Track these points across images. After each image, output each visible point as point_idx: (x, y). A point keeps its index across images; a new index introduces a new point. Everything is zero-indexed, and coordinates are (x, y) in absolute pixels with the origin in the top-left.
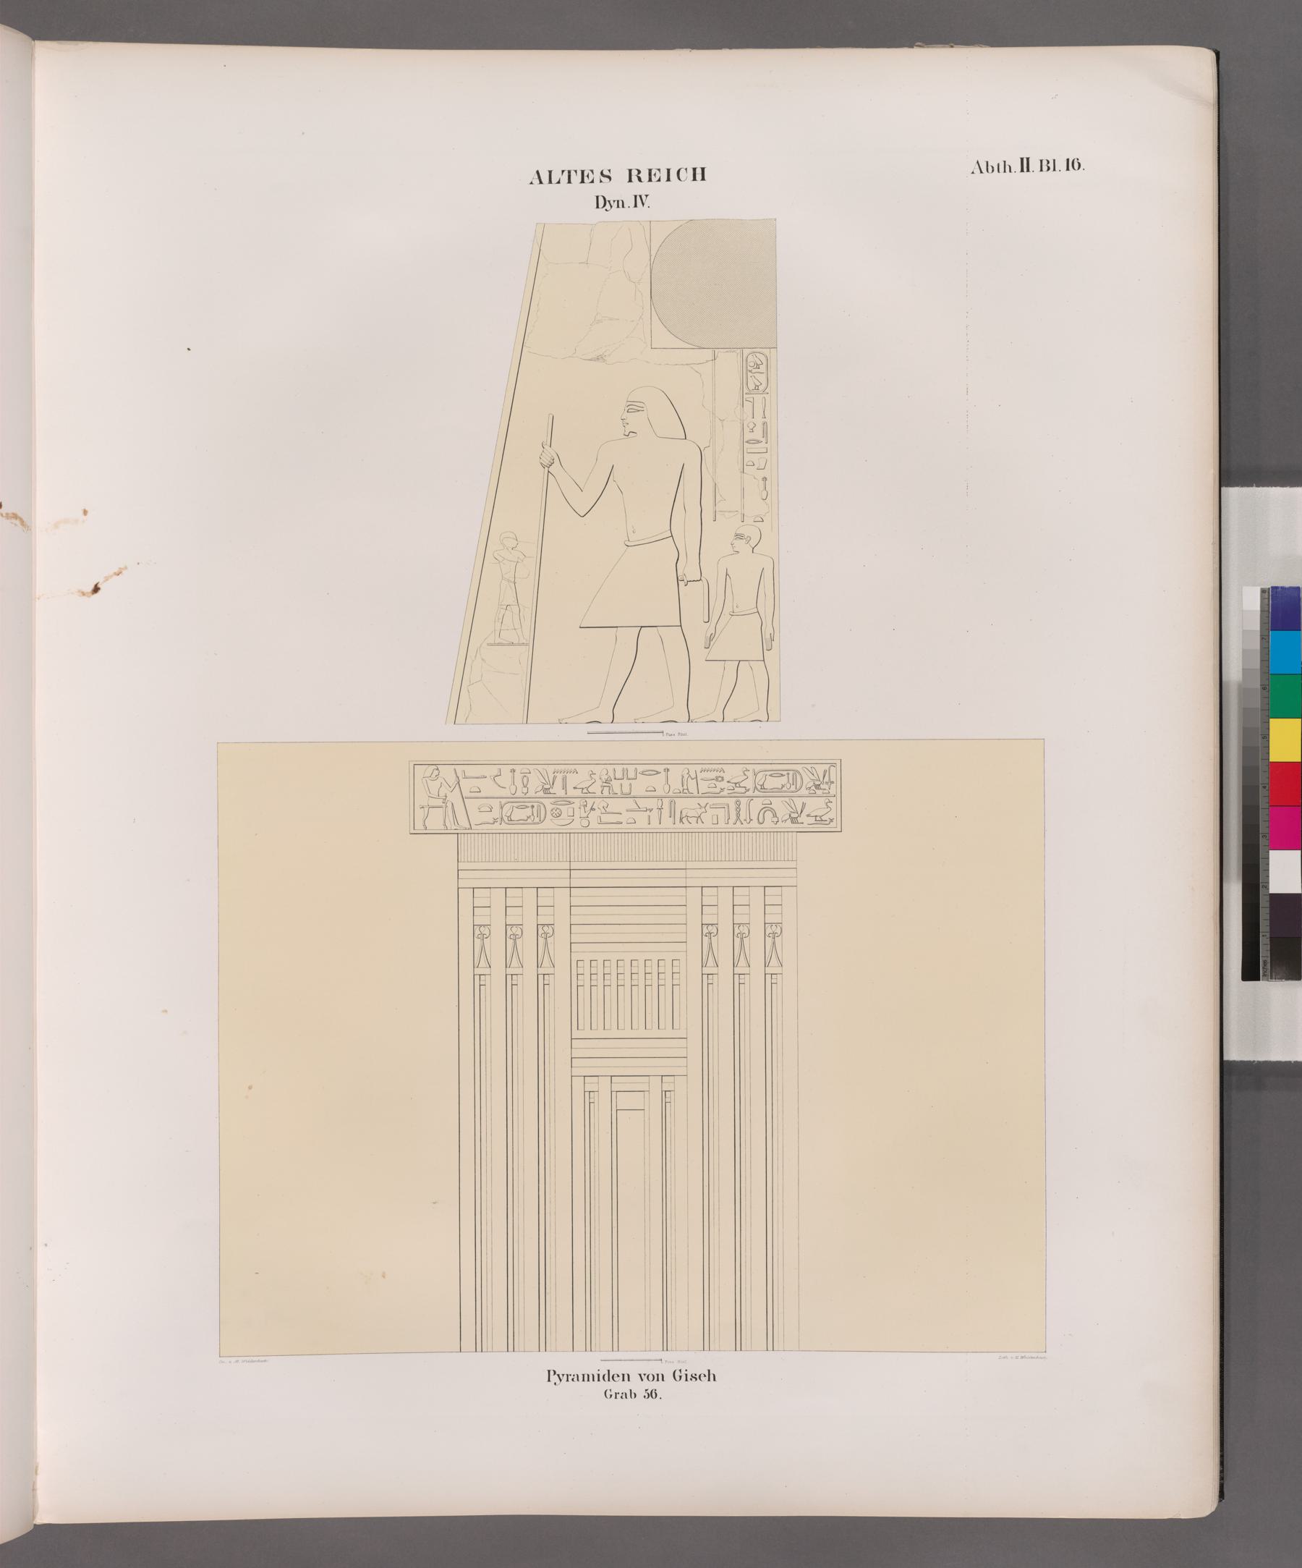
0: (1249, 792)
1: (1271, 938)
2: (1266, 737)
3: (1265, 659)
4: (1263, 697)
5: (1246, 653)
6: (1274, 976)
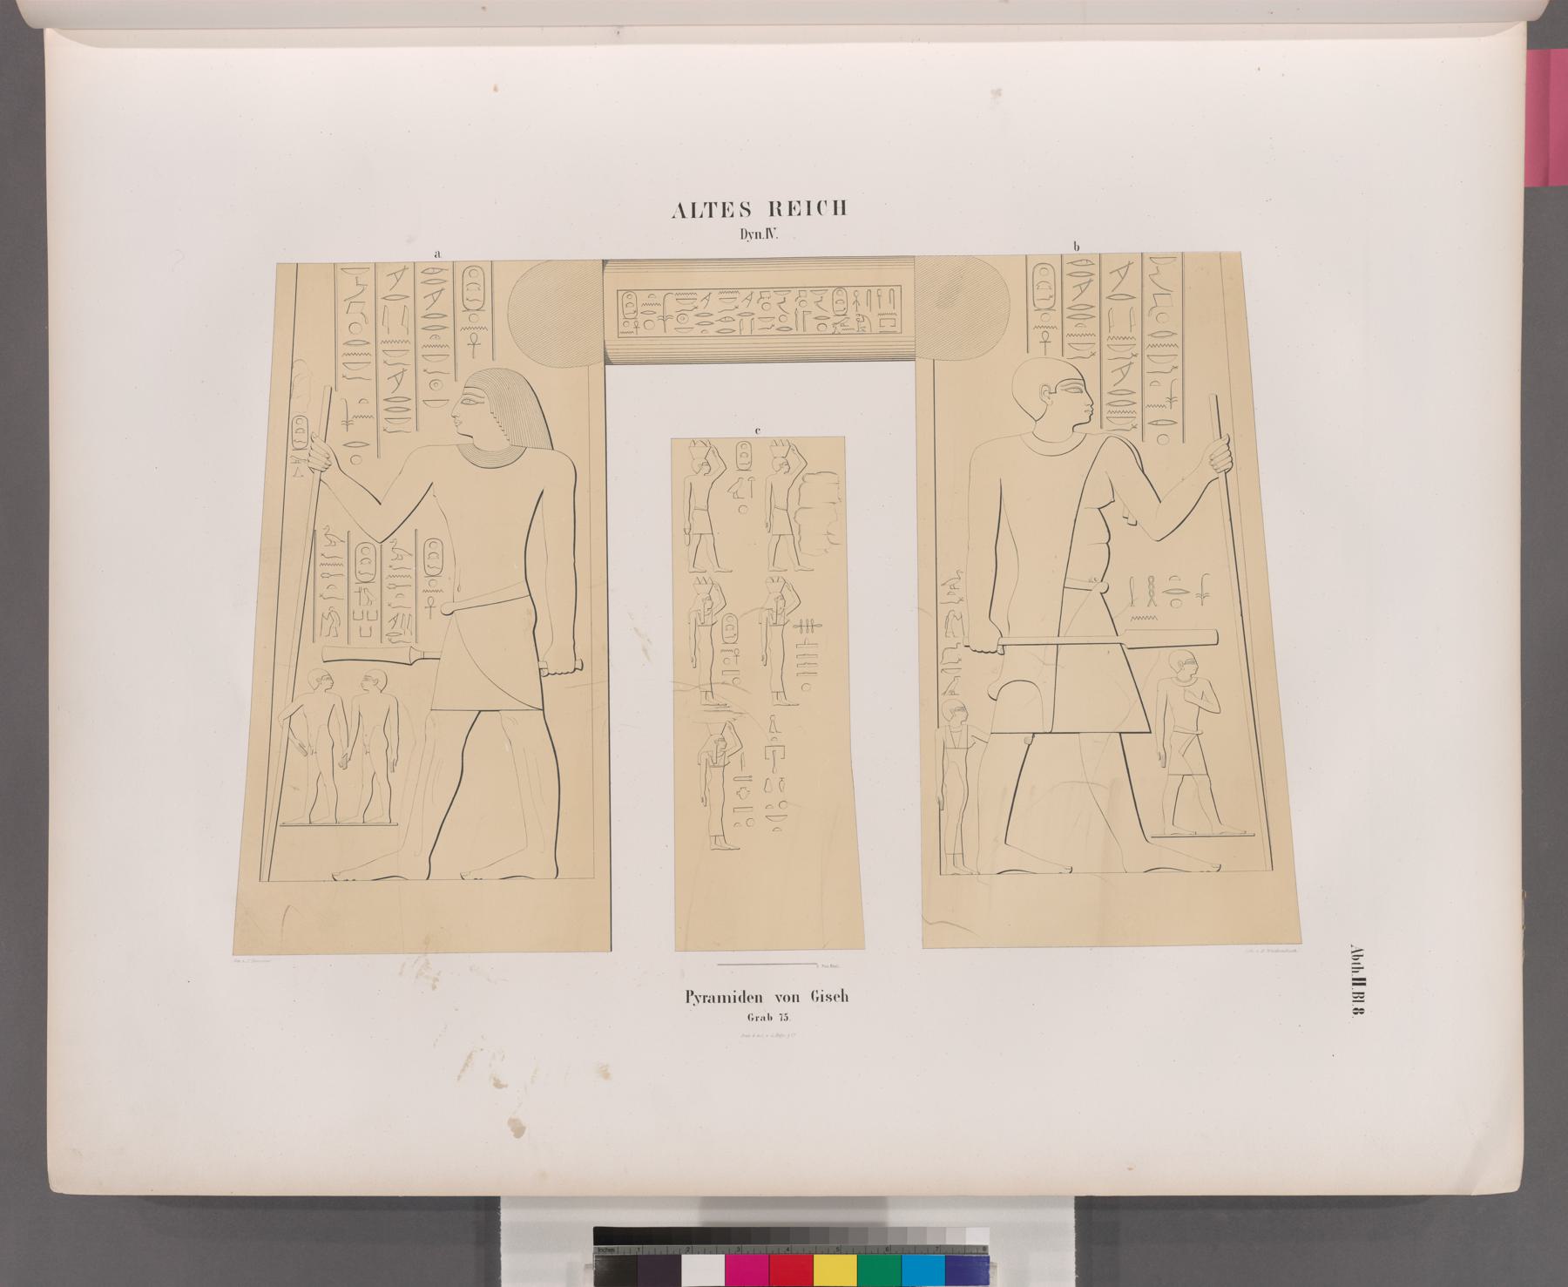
1: (635, 1259)
2: (838, 1251)
4: (878, 1248)
5: (923, 1231)
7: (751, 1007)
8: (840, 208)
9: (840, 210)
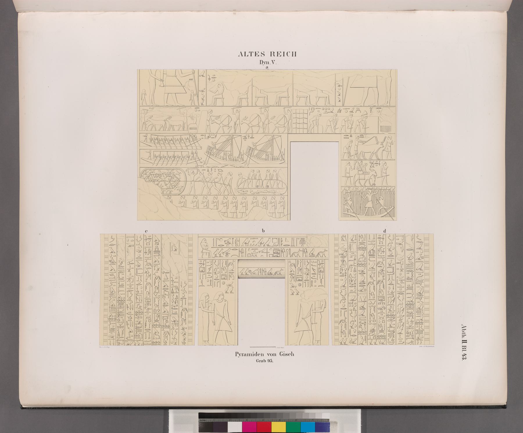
0: (262, 415)
2: (280, 421)
3: (305, 420)
5: (308, 413)
6: (200, 423)
7: (260, 358)
8: (294, 54)
9: (294, 55)
